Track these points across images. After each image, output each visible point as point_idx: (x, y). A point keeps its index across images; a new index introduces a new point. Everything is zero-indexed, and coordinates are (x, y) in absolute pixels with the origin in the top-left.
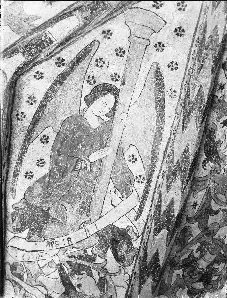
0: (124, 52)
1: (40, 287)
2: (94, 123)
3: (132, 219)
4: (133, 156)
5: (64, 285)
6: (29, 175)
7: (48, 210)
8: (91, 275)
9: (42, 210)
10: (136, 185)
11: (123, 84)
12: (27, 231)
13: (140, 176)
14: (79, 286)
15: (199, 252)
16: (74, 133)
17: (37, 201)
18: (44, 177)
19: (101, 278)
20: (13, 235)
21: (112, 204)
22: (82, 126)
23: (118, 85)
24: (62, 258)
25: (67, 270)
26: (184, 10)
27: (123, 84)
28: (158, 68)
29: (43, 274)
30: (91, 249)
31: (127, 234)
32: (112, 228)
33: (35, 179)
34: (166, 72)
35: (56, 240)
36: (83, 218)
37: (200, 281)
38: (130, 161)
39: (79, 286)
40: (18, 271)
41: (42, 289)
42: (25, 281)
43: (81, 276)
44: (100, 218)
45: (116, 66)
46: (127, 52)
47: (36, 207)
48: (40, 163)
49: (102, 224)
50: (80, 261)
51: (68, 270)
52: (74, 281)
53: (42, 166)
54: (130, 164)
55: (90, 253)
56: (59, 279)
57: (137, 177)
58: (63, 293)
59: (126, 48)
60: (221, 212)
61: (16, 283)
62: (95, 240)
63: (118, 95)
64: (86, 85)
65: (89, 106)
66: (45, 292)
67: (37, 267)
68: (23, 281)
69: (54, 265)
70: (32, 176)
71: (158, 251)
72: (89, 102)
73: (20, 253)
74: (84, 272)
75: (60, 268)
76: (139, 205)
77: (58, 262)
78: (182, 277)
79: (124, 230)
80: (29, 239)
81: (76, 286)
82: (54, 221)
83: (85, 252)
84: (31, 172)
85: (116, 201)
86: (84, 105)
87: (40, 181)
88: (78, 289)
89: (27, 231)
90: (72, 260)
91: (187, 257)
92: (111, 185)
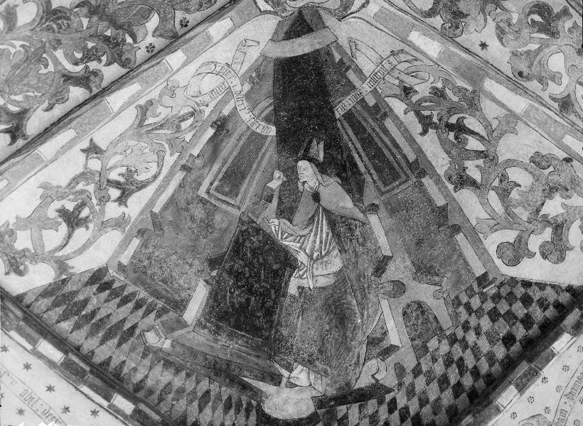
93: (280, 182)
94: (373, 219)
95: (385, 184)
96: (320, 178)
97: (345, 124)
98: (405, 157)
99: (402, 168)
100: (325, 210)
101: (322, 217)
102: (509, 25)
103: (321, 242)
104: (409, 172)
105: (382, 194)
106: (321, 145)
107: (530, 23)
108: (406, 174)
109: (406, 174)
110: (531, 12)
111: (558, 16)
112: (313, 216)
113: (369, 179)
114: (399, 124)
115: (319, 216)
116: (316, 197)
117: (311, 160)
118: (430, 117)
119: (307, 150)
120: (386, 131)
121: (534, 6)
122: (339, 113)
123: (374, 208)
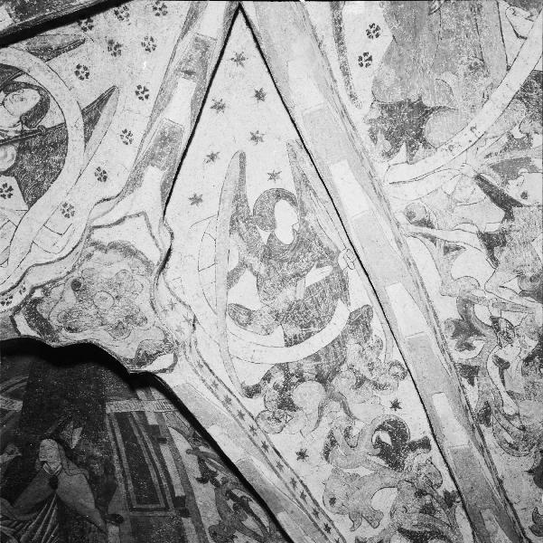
1: (461, 226)
5: (501, 205)
6: (365, 60)
7: (420, 98)
9: (411, 105)
12: (403, 148)
14: (524, 195)
17: (398, 96)
18: (389, 52)
20: (385, 166)
24: (476, 163)
25: (495, 180)
29: (458, 204)
30: (517, 127)
33: (376, 61)
35: (455, 140)
36: (483, 82)
39: (524, 195)
40: (419, 216)
41: (468, 227)
42: (436, 226)
43: (520, 179)
44: (508, 69)
47: (400, 104)
48: (373, 31)
50: (508, 156)
51: (494, 178)
53: (377, 36)
56: (488, 199)
58: (503, 220)
61: (425, 236)
66: (475, 229)
67: (444, 196)
70: (370, 59)
73: (409, 188)
74: (523, 170)
77: (473, 174)
80: (411, 160)
81: (520, 198)
83: (511, 137)
84: (365, 54)
87: (388, 58)
89: (403, 148)
90: (493, 160)
93: (13, 456)
94: (113, 529)
95: (139, 501)
96: (65, 462)
97: (115, 424)
98: (172, 488)
99: (164, 497)
100: (58, 499)
101: (54, 506)
102: (347, 435)
103: (43, 532)
104: (171, 505)
105: (132, 509)
106: (78, 431)
107: (374, 441)
108: (166, 504)
109: (166, 504)
110: (381, 428)
111: (413, 447)
112: (42, 504)
113: (121, 485)
114: (175, 451)
115: (49, 505)
116: (54, 482)
117: (59, 441)
118: (215, 474)
119: (58, 431)
120: (159, 454)
121: (389, 422)
122: (111, 408)
123: (118, 520)
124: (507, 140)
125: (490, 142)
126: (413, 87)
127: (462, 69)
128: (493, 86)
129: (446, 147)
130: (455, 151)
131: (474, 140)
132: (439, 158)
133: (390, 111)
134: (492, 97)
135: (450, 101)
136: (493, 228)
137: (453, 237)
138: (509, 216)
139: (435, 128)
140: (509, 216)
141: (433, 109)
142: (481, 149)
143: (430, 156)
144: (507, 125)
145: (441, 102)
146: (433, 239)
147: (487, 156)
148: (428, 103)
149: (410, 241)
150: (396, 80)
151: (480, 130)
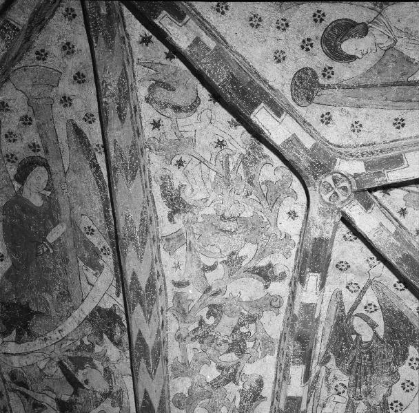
0: (30, 119)
1: (47, 392)
2: (37, 201)
3: (114, 296)
4: (89, 228)
7: (28, 304)
8: (94, 367)
9: (21, 306)
10: (104, 257)
11: (47, 152)
13: (104, 247)
15: (212, 318)
16: (20, 217)
19: (105, 370)
21: (89, 283)
22: (26, 207)
23: (41, 154)
25: (71, 368)
26: (73, 52)
27: (47, 152)
28: (75, 125)
31: (115, 314)
32: (98, 309)
34: (84, 127)
36: (67, 305)
37: (229, 351)
38: (88, 233)
39: (87, 382)
43: (85, 371)
44: (83, 301)
45: (31, 135)
46: (34, 119)
49: (87, 308)
52: (80, 377)
54: (89, 237)
55: (88, 343)
57: (102, 249)
59: (30, 114)
60: (220, 266)
61: (23, 393)
62: (88, 330)
63: (48, 166)
64: (9, 166)
65: (23, 185)
66: (54, 396)
67: (38, 370)
68: (28, 389)
69: (54, 364)
71: (140, 331)
72: (22, 177)
73: (15, 359)
75: (61, 364)
76: (115, 279)
78: (200, 351)
79: (111, 310)
80: (18, 341)
81: (83, 383)
82: (39, 314)
83: (82, 342)
85: (93, 279)
86: (17, 185)
88: (85, 386)
90: (70, 354)
91: (197, 326)
92: (81, 263)
124: (79, 344)
125: (69, 342)
126: (23, 296)
127: (55, 294)
128: (74, 308)
129: (43, 338)
130: (48, 342)
131: (60, 338)
132: (37, 345)
133: (8, 307)
134: (73, 314)
135: (47, 310)
136: (66, 398)
137: (39, 398)
138: (76, 393)
139: (37, 325)
140: (76, 393)
141: (36, 313)
142: (64, 346)
143: (32, 341)
144: (80, 334)
145: (41, 309)
146: (27, 396)
147: (67, 351)
148: (34, 308)
149: (11, 394)
150: (12, 290)
151: (65, 333)
